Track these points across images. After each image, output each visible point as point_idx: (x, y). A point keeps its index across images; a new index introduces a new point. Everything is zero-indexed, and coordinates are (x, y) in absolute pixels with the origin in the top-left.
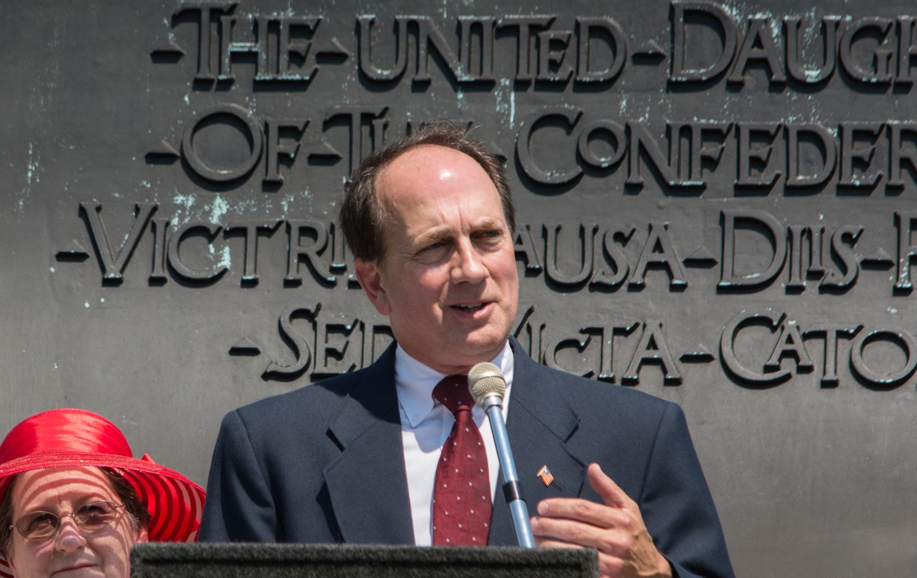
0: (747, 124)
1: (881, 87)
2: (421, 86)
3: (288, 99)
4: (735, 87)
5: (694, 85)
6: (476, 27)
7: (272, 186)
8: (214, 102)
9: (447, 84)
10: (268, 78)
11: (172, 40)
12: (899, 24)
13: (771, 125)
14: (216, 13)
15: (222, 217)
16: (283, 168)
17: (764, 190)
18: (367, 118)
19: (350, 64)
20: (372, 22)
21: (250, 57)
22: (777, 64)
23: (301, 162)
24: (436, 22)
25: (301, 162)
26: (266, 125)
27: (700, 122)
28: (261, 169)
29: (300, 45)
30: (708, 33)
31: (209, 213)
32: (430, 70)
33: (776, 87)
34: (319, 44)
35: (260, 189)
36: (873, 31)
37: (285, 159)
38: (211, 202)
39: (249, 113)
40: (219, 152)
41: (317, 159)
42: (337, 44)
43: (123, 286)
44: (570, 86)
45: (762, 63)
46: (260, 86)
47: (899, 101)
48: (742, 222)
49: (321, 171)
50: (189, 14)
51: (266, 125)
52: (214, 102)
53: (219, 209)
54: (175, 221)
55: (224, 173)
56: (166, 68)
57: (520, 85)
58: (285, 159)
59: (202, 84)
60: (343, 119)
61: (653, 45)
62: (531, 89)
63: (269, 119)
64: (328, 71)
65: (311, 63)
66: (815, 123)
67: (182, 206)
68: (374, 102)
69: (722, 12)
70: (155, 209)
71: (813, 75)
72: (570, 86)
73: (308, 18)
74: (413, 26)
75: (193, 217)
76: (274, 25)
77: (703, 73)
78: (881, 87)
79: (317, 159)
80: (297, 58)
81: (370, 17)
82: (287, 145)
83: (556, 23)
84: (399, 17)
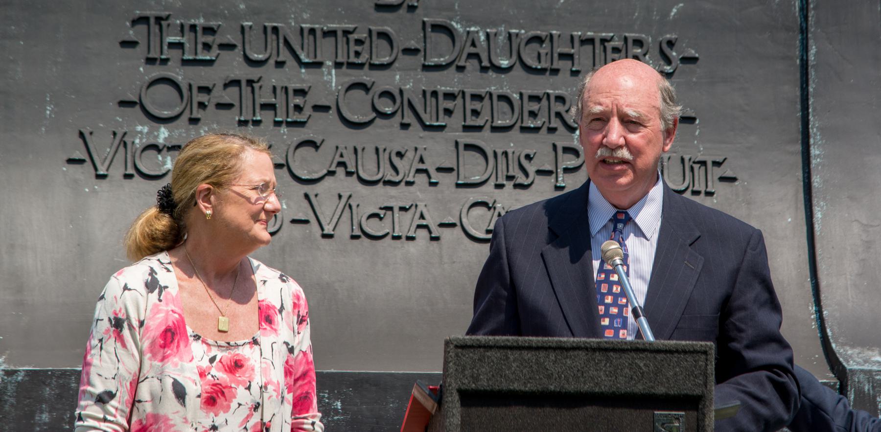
0: (469, 91)
1: (542, 71)
2: (280, 64)
3: (202, 70)
4: (461, 69)
5: (438, 67)
6: (312, 31)
7: (194, 121)
8: (157, 72)
9: (295, 64)
10: (191, 57)
11: (131, 34)
12: (551, 36)
13: (482, 91)
14: (159, 19)
15: (165, 139)
16: (201, 111)
17: (479, 128)
18: (250, 82)
19: (239, 51)
20: (251, 27)
21: (180, 45)
22: (484, 56)
23: (211, 108)
24: (289, 27)
25: (211, 108)
26: (190, 86)
27: (442, 89)
28: (187, 111)
29: (209, 39)
30: (444, 38)
31: (157, 137)
32: (285, 55)
33: (484, 69)
34: (219, 39)
35: (187, 123)
36: (538, 39)
37: (202, 105)
38: (158, 130)
39: (179, 79)
40: (162, 100)
41: (220, 106)
42: (229, 38)
43: (108, 179)
44: (367, 66)
45: (476, 56)
46: (185, 62)
47: (553, 79)
48: (469, 147)
49: (223, 113)
50: (144, 20)
51: (190, 86)
52: (157, 72)
53: (163, 134)
54: (137, 141)
55: (166, 113)
56: (128, 51)
57: (338, 65)
58: (202, 105)
59: (150, 61)
60: (236, 83)
61: (413, 44)
62: (344, 67)
63: (192, 82)
64: (225, 54)
65: (215, 51)
66: (506, 91)
67: (141, 132)
68: (254, 73)
69: (452, 25)
70: (125, 134)
71: (505, 63)
72: (367, 66)
73: (213, 23)
74: (275, 30)
75: (148, 139)
76: (193, 27)
77: (442, 60)
78: (542, 71)
79: (220, 106)
80: (207, 47)
81: (250, 23)
82: (203, 98)
83: (357, 30)
84: (267, 24)
